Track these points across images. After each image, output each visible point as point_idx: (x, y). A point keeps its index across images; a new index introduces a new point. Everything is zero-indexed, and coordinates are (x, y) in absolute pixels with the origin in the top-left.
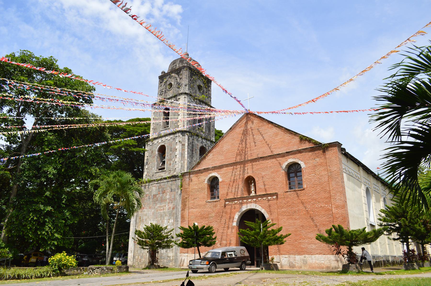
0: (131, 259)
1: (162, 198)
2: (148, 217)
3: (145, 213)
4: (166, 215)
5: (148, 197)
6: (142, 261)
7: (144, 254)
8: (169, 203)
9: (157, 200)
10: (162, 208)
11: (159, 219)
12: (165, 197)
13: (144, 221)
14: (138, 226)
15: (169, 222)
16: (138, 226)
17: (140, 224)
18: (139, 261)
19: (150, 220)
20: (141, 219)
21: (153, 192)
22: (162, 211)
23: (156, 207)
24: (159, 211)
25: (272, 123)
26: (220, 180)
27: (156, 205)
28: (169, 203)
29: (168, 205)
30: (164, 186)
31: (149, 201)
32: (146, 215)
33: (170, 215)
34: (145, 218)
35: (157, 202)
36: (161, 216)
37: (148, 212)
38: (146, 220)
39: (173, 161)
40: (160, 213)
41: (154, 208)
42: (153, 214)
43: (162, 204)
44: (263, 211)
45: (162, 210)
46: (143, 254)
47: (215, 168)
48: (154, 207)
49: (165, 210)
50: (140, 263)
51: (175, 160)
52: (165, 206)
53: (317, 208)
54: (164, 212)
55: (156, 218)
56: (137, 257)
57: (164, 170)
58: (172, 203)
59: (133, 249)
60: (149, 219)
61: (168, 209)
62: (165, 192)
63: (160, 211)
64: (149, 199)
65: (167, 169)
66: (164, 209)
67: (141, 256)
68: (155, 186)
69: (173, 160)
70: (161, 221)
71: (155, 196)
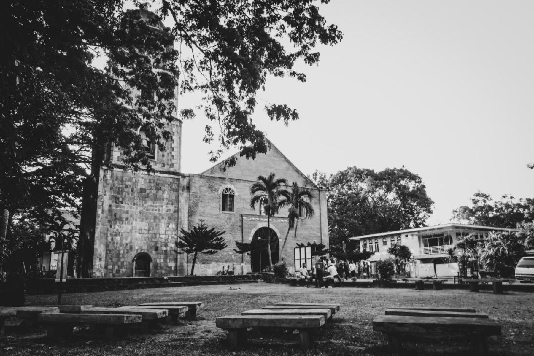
0: (100, 269)
1: (155, 195)
2: (131, 216)
3: (126, 209)
4: (163, 218)
5: (130, 189)
6: (121, 272)
7: (125, 263)
8: (167, 204)
9: (147, 196)
10: (157, 208)
11: (152, 221)
12: (160, 195)
13: (124, 219)
14: (111, 226)
15: (168, 227)
16: (111, 226)
17: (116, 223)
18: (114, 272)
19: (136, 221)
20: (118, 216)
21: (139, 184)
22: (155, 212)
23: (146, 205)
24: (151, 211)
25: (285, 158)
26: (236, 194)
27: (145, 203)
28: (167, 204)
29: (167, 207)
30: (159, 182)
31: (132, 195)
32: (127, 212)
33: (170, 218)
34: (124, 216)
35: (147, 199)
36: (155, 218)
37: (131, 208)
38: (127, 219)
39: (168, 154)
40: (154, 213)
41: (143, 205)
42: (140, 213)
43: (156, 203)
44: (276, 231)
45: (156, 210)
46: (122, 263)
47: (231, 180)
48: (141, 204)
49: (162, 211)
50: (117, 274)
51: (171, 153)
52: (162, 206)
53: (312, 234)
54: (160, 214)
55: (147, 219)
56: (110, 267)
57: (153, 160)
58: (172, 204)
59: (105, 256)
60: (133, 218)
61: (167, 211)
62: (161, 189)
63: (153, 210)
64: (132, 191)
65: (157, 160)
66: (159, 210)
67: (119, 266)
68: (142, 178)
69: (168, 151)
70: (155, 224)
71: (142, 190)
